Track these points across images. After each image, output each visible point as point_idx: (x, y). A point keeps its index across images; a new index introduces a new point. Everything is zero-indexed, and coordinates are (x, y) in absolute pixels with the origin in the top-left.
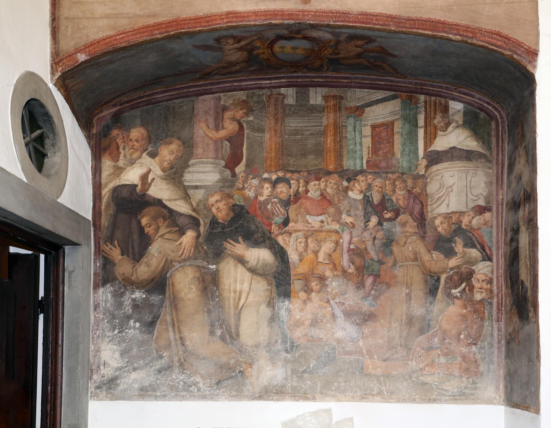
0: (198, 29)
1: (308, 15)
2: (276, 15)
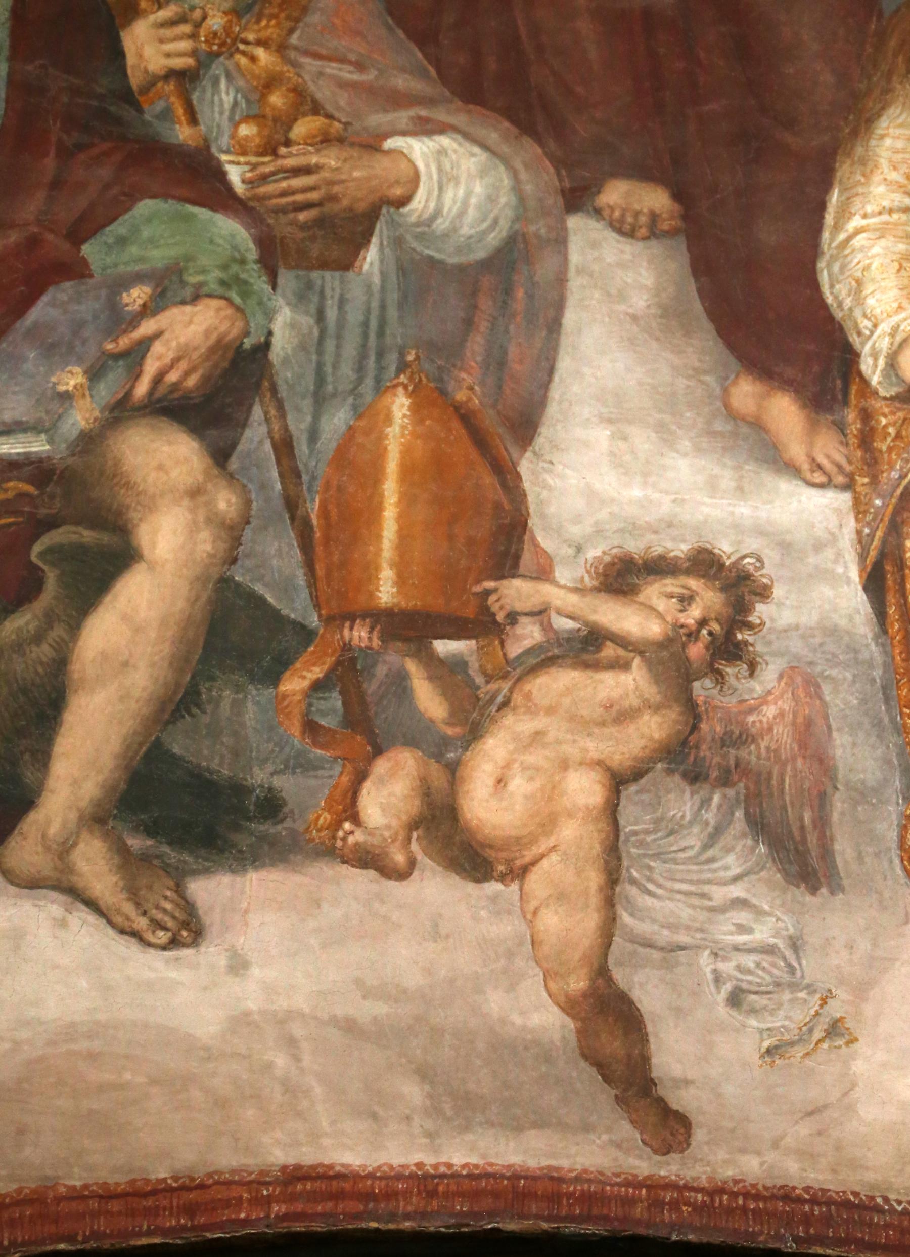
0: (144, 1241)
1: (675, 1205)
2: (525, 1196)
